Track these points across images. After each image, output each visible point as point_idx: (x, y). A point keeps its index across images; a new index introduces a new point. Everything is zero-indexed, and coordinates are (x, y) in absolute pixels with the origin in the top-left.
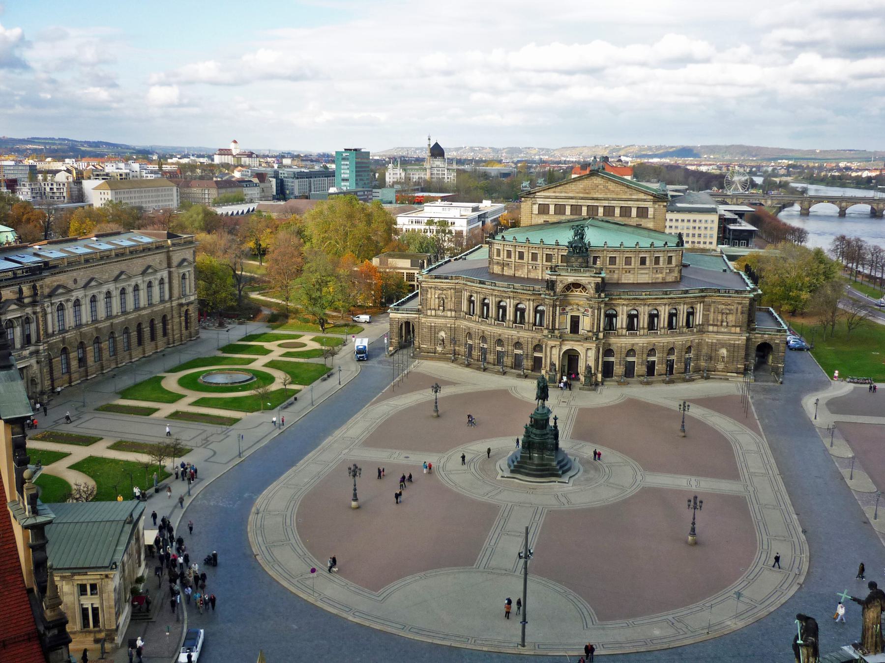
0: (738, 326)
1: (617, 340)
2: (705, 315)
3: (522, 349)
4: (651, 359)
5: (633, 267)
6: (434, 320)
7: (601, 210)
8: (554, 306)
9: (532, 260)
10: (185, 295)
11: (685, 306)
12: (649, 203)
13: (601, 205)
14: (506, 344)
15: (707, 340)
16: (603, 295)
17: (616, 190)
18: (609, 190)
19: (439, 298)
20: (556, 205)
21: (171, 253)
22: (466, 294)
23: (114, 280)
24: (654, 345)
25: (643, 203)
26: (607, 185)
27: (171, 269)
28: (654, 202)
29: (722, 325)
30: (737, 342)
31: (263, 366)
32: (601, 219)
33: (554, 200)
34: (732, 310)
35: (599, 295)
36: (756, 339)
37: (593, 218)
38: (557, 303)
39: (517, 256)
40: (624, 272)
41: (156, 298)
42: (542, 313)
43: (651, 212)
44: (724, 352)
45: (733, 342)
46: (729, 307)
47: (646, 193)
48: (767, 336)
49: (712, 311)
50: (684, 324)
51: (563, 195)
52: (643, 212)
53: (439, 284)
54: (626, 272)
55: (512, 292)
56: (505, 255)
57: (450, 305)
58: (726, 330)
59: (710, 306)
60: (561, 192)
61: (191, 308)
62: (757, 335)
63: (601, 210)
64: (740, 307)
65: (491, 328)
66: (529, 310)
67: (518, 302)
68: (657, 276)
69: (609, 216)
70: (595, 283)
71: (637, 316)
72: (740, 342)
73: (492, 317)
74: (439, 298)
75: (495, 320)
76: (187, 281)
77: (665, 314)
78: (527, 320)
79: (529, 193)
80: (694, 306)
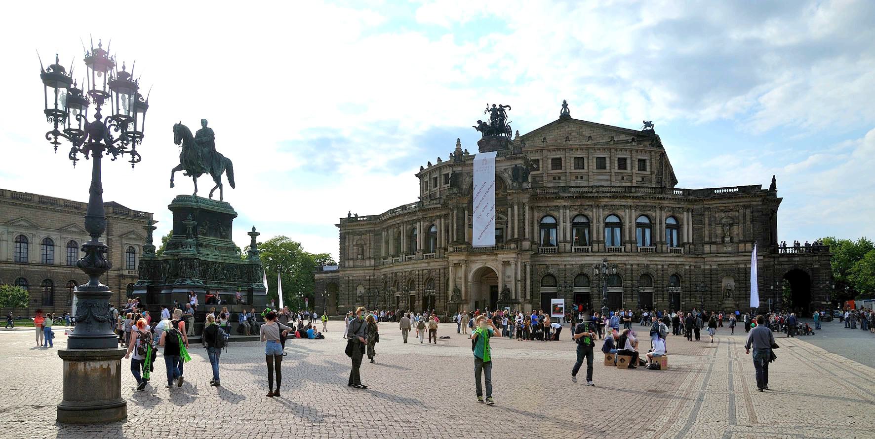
1: (558, 259)
5: (587, 171)
6: (352, 272)
11: (663, 212)
15: (702, 267)
26: (581, 130)
29: (723, 242)
34: (738, 218)
40: (574, 178)
45: (743, 266)
46: (730, 214)
48: (797, 259)
49: (707, 222)
58: (730, 249)
59: (703, 215)
62: (781, 259)
64: (748, 212)
65: (402, 267)
66: (441, 231)
67: (427, 223)
70: (512, 168)
71: (588, 225)
74: (357, 245)
80: (677, 215)
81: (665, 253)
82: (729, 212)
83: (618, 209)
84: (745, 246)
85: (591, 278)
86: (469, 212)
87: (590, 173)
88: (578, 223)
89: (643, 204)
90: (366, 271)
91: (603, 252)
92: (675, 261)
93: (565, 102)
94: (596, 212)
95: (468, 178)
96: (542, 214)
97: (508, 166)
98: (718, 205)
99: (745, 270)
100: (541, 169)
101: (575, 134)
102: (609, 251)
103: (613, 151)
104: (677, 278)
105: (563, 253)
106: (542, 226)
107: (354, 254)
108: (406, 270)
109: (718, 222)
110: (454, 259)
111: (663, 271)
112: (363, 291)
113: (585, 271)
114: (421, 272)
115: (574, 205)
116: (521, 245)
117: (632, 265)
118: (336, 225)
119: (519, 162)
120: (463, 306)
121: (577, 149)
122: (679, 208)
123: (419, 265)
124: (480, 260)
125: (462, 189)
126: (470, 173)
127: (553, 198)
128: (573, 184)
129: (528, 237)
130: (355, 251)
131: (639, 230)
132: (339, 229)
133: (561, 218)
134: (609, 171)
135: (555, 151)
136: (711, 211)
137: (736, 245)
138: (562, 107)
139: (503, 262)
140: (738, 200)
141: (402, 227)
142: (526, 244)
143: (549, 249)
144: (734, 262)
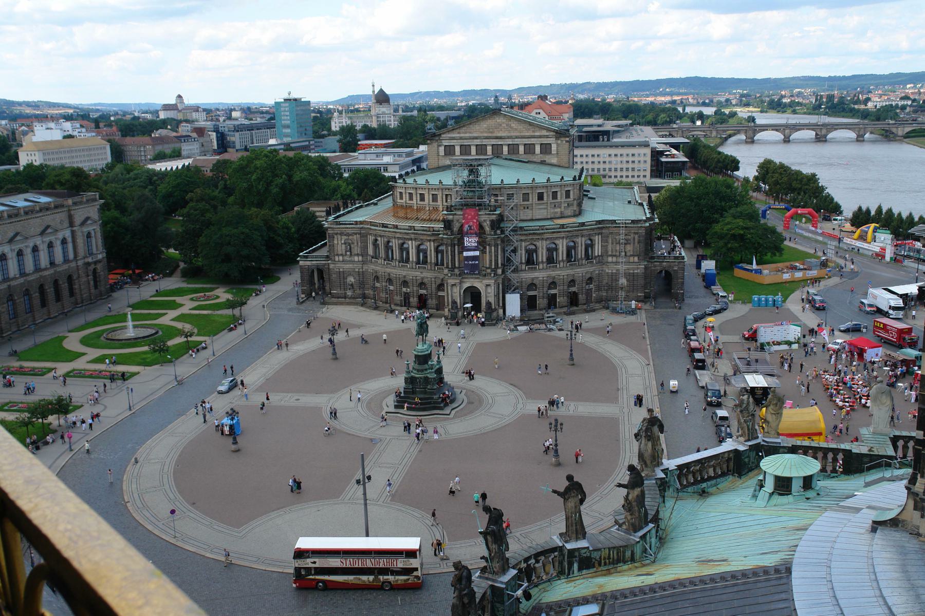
0: (635, 256)
2: (604, 246)
3: (426, 289)
4: (553, 292)
7: (505, 149)
8: (453, 246)
9: (433, 201)
10: (91, 254)
12: (552, 139)
13: (505, 143)
14: (410, 284)
15: (607, 271)
16: (499, 232)
17: (519, 127)
18: (511, 127)
20: (461, 146)
21: (72, 212)
22: (371, 239)
23: (8, 242)
24: (554, 278)
25: (545, 139)
27: (74, 228)
28: (557, 138)
30: (636, 271)
31: (172, 320)
32: (504, 157)
33: (459, 141)
35: (495, 233)
36: (655, 267)
37: (498, 157)
38: (456, 242)
39: (418, 198)
40: (522, 208)
41: (59, 257)
42: (442, 252)
43: (554, 147)
44: (623, 281)
45: (632, 271)
47: (548, 130)
48: (665, 264)
49: (610, 242)
50: (583, 256)
51: (467, 135)
52: (546, 149)
54: (524, 208)
55: (413, 233)
56: (408, 198)
57: (357, 250)
60: (466, 133)
61: (99, 266)
62: (656, 263)
63: (505, 149)
64: (636, 236)
65: (396, 271)
66: (431, 251)
67: (419, 243)
68: (556, 210)
69: (514, 153)
70: (490, 220)
71: (536, 251)
73: (396, 259)
75: (399, 262)
76: (93, 240)
77: (563, 247)
78: (429, 261)
79: (434, 135)
80: (592, 238)
85: (538, 286)
87: (534, 205)
103: (549, 188)
104: (590, 280)
112: (353, 280)
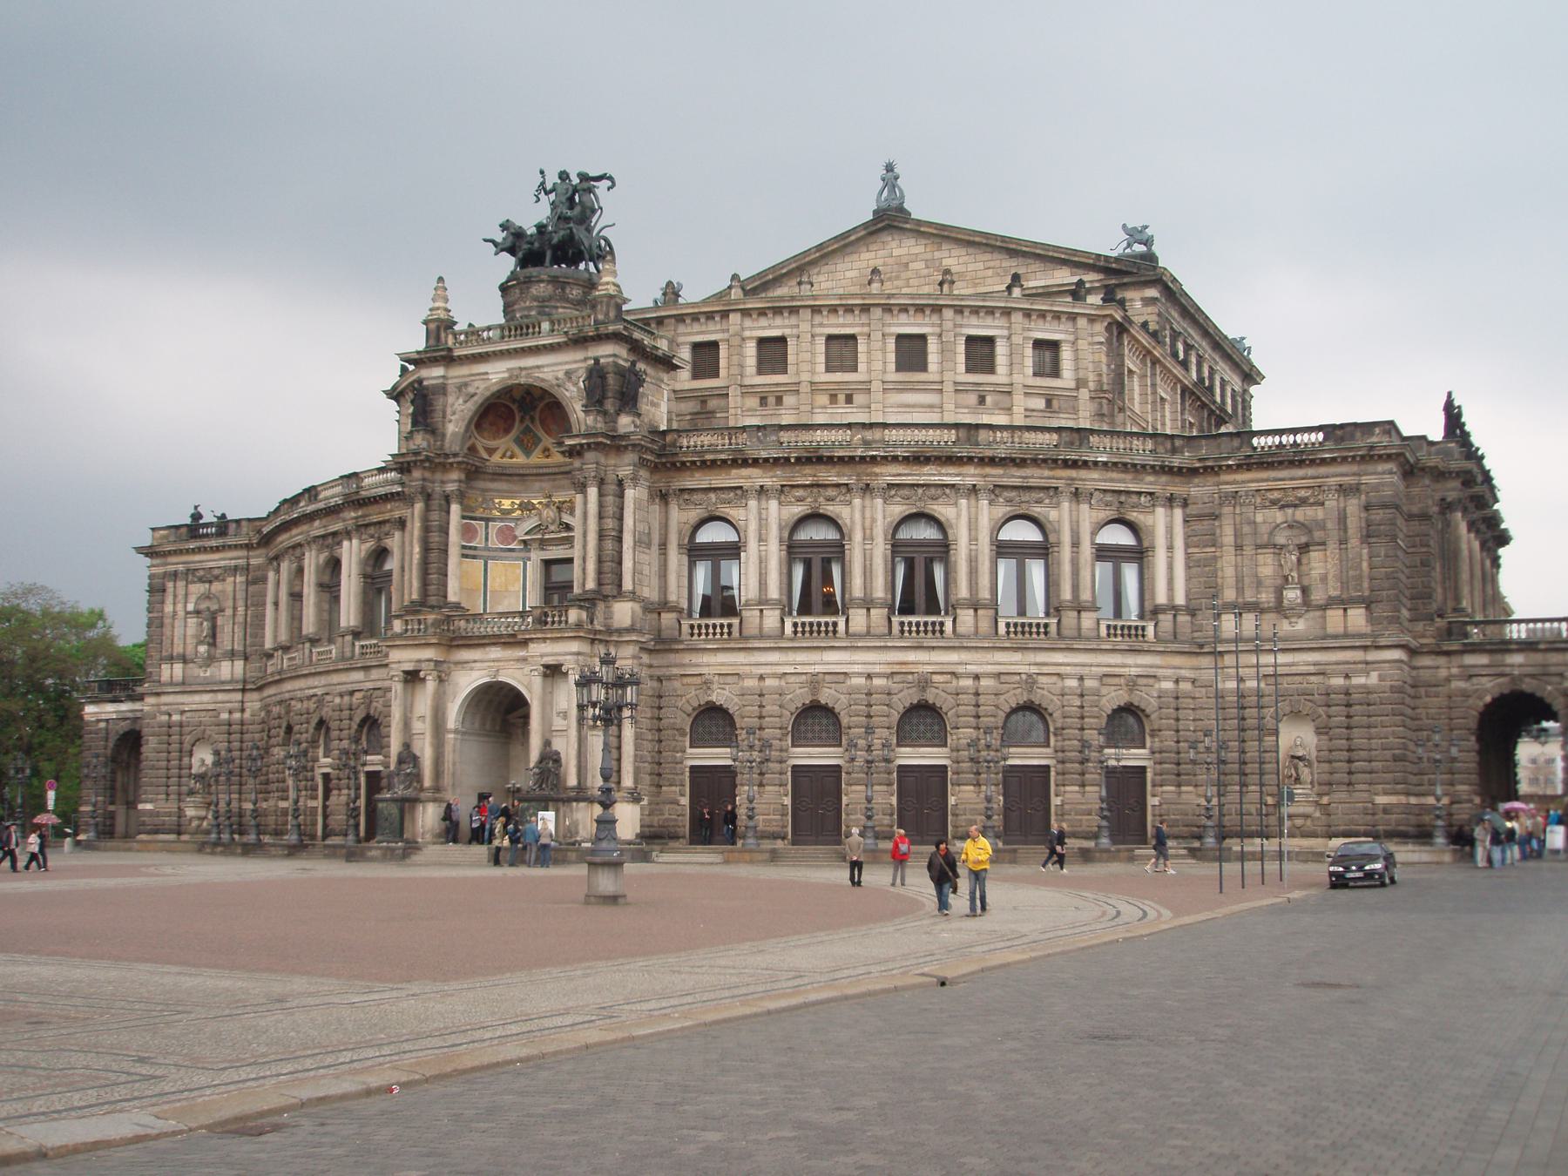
1: (741, 658)
19: (197, 612)
24: (924, 682)
30: (1358, 680)
34: (1322, 526)
40: (823, 399)
44: (1296, 737)
45: (1338, 681)
46: (1301, 514)
48: (1518, 659)
49: (1228, 539)
53: (197, 558)
57: (229, 636)
59: (1216, 517)
62: (1470, 660)
64: (1353, 506)
67: (370, 545)
72: (1373, 679)
74: (197, 612)
77: (973, 539)
80: (1133, 516)
81: (1088, 639)
82: (1295, 506)
83: (934, 498)
84: (1345, 615)
85: (845, 721)
86: (463, 510)
88: (813, 544)
89: (1017, 482)
90: (220, 697)
91: (880, 637)
92: (1124, 666)
93: (889, 168)
94: (864, 507)
95: (461, 401)
96: (694, 515)
97: (576, 362)
98: (1264, 485)
99: (1347, 694)
100: (723, 372)
101: (922, 265)
102: (902, 632)
105: (754, 638)
106: (696, 552)
107: (189, 640)
108: (311, 692)
109: (1266, 537)
110: (403, 658)
111: (1082, 696)
112: (209, 759)
113: (825, 697)
114: (346, 698)
115: (793, 486)
116: (609, 616)
117: (977, 677)
118: (139, 550)
119: (607, 352)
120: (424, 808)
121: (833, 309)
122: (1140, 493)
123: (343, 678)
124: (482, 661)
125: (444, 435)
126: (466, 385)
127: (724, 461)
128: (820, 419)
129: (631, 588)
130: (191, 631)
131: (1006, 567)
132: (148, 561)
133: (753, 527)
134: (937, 378)
135: (766, 314)
136: (1241, 505)
137: (1318, 613)
138: (881, 184)
139: (546, 666)
140: (1323, 470)
141: (307, 554)
142: (623, 612)
143: (722, 626)
144: (1312, 669)
